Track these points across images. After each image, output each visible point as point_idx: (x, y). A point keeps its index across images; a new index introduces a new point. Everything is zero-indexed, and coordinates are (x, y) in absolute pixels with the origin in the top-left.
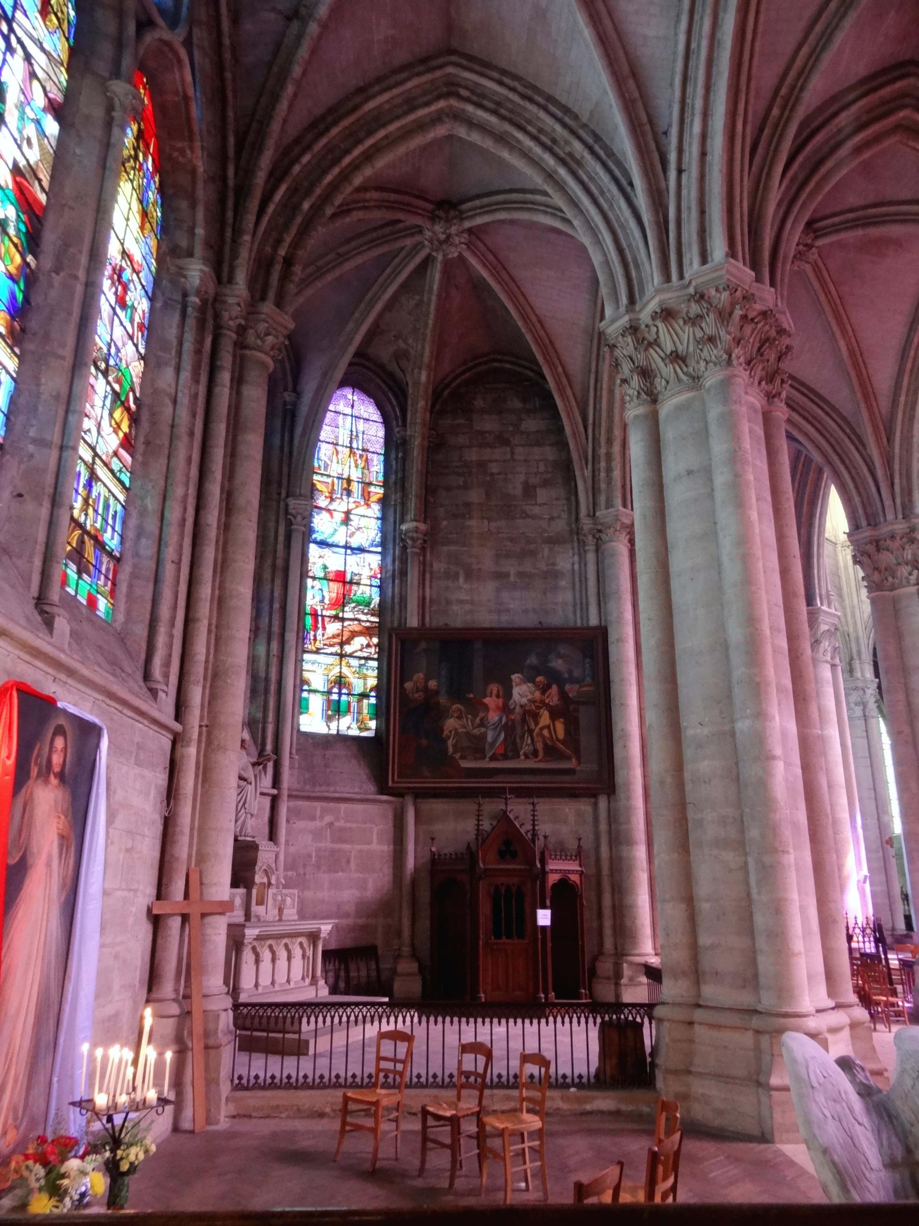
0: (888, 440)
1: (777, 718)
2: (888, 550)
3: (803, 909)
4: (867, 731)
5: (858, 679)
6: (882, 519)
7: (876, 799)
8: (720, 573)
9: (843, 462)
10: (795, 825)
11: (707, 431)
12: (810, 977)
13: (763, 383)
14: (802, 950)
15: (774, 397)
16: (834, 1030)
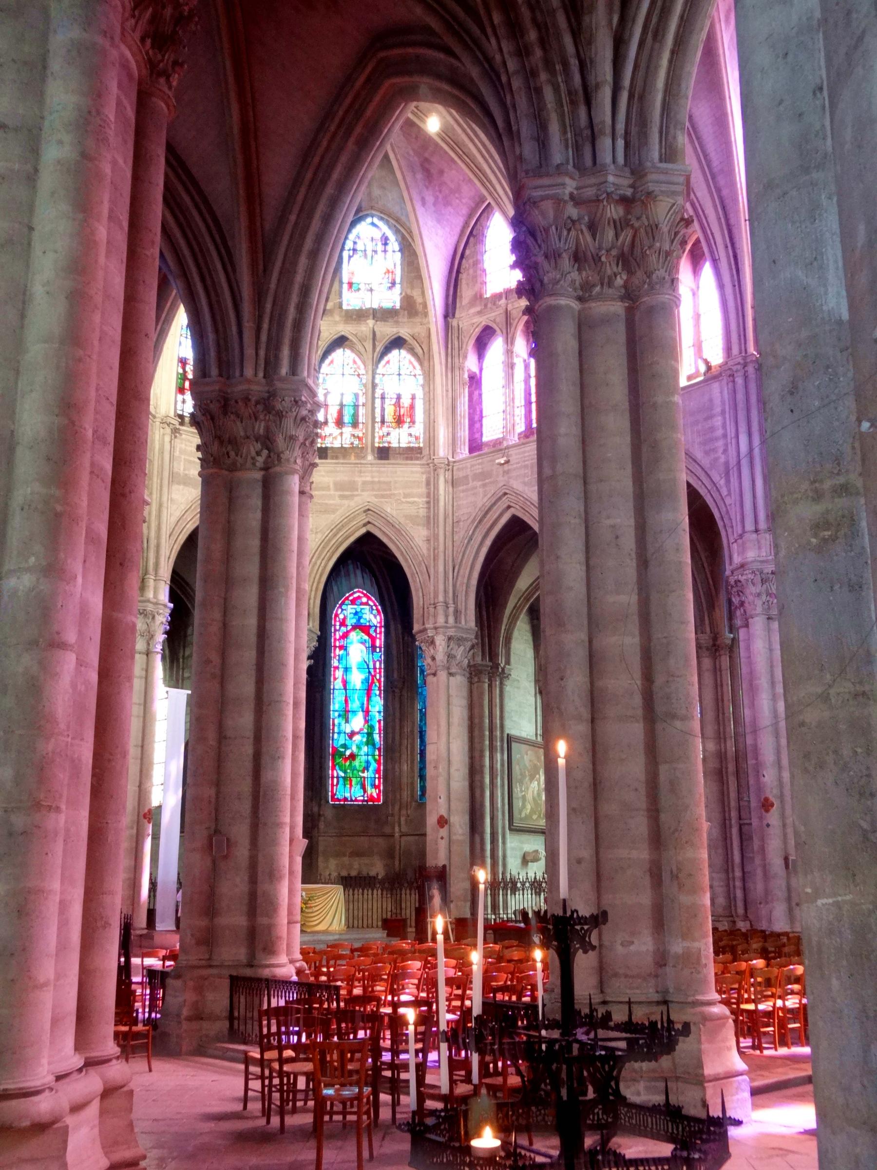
0: (265, 271)
1: (80, 580)
2: (238, 416)
3: (63, 906)
4: (147, 671)
5: (148, 601)
6: (237, 374)
7: (142, 759)
8: (23, 316)
9: (203, 280)
10: (75, 765)
11: (45, 68)
12: (55, 1022)
13: (149, 42)
14: (52, 976)
15: (160, 74)
16: (77, 1108)
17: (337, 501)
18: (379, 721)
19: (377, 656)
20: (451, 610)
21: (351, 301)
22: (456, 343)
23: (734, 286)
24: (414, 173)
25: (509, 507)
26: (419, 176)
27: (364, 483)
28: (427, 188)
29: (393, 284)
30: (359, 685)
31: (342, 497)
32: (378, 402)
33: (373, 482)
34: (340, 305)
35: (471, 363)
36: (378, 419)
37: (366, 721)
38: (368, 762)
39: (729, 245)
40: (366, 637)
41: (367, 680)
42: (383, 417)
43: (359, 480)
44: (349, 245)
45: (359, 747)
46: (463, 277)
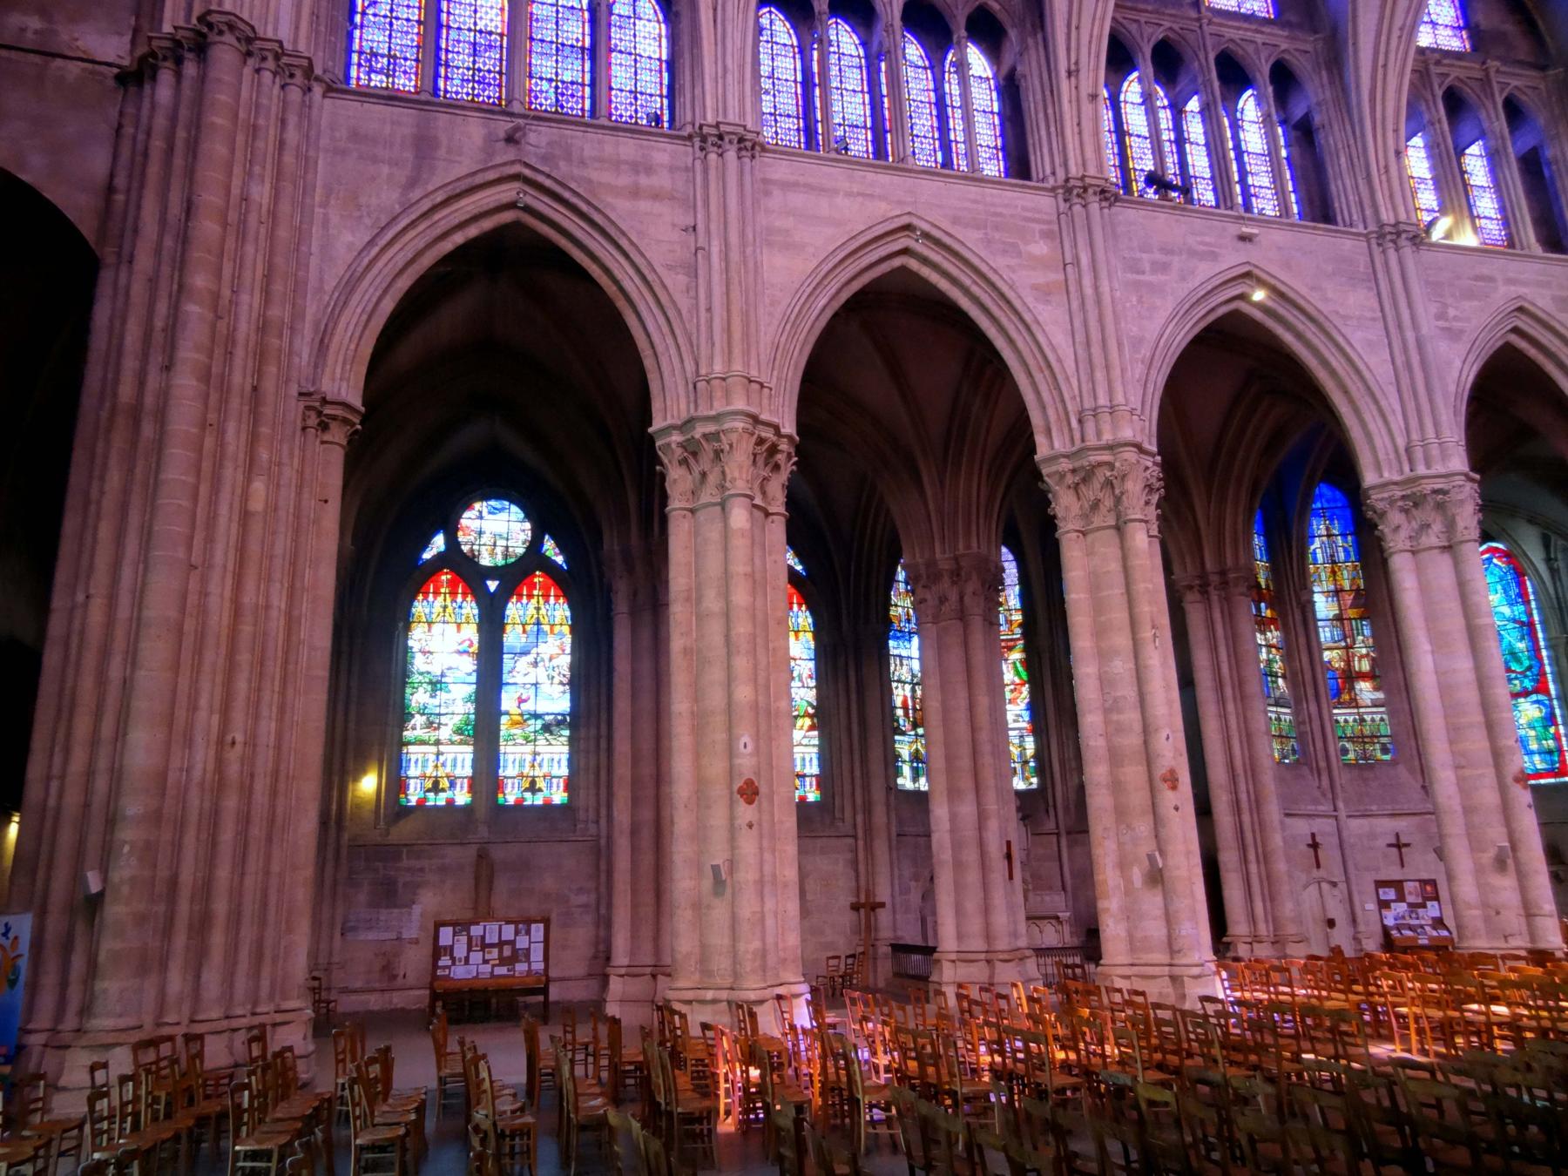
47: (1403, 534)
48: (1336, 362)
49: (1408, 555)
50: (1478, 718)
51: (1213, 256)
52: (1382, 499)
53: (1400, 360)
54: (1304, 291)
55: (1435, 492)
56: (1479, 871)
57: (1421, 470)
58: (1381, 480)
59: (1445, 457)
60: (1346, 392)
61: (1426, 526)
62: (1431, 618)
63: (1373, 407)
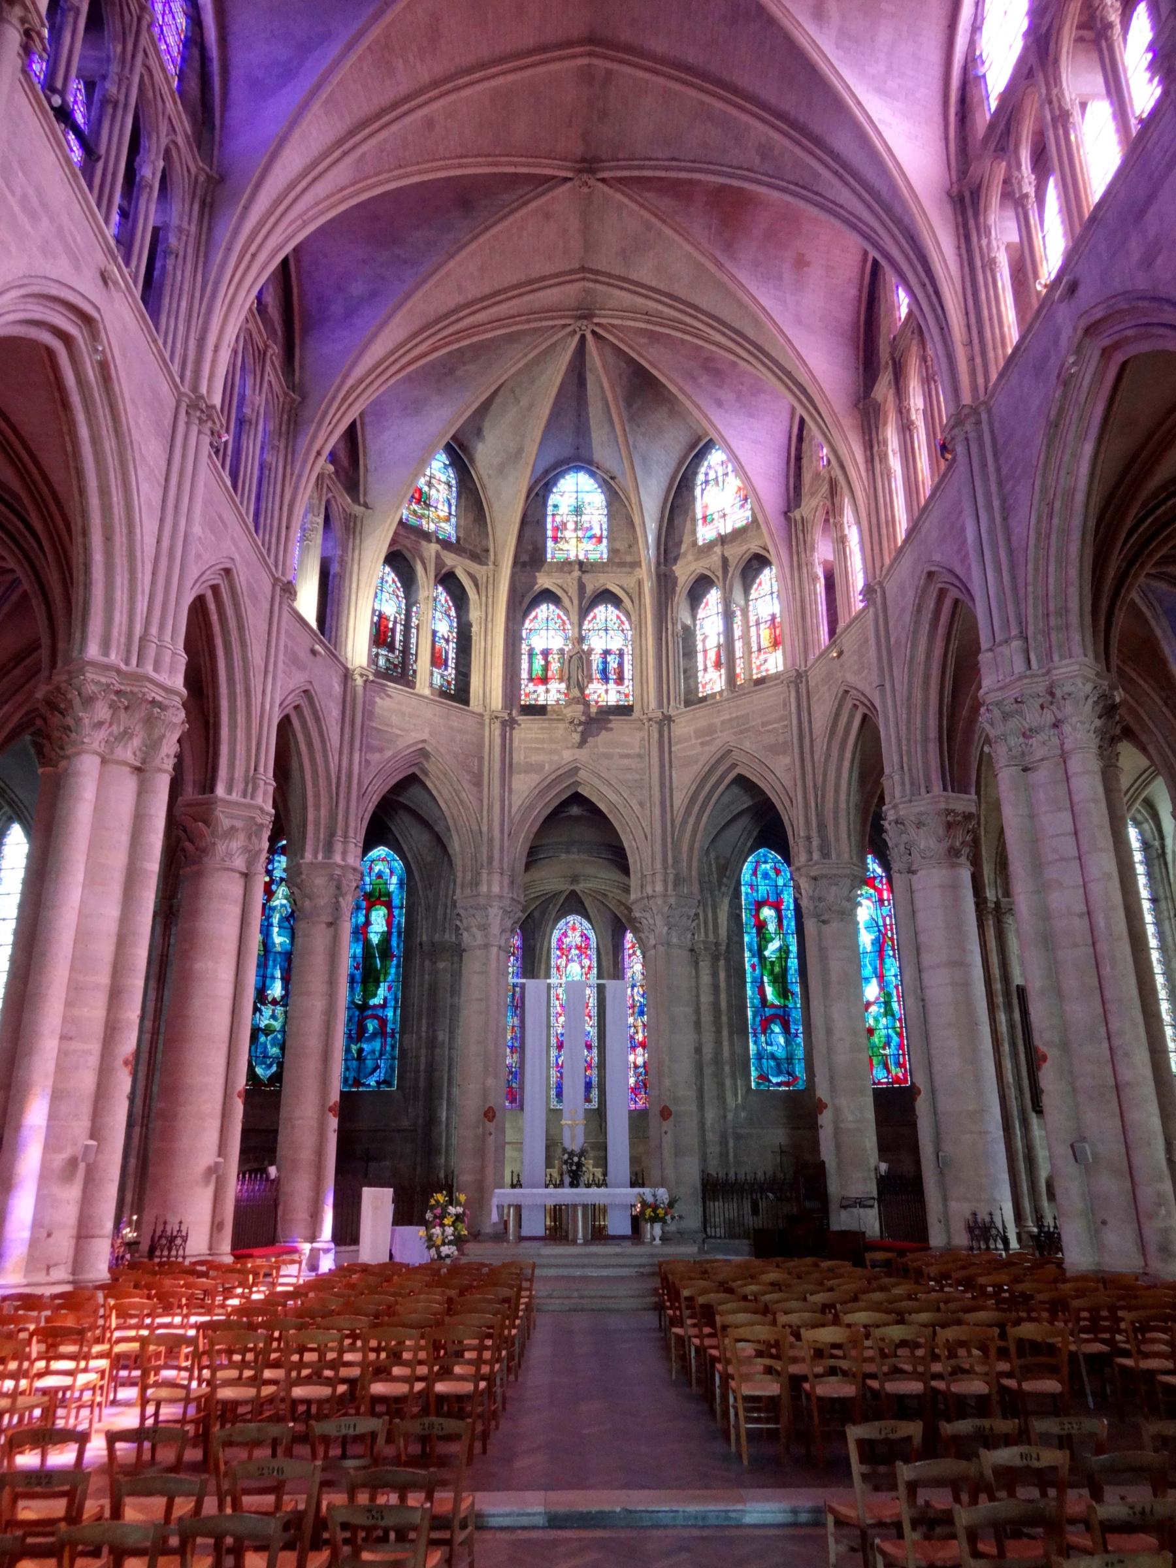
17: (699, 749)
18: (896, 987)
19: (885, 911)
20: (816, 842)
21: (705, 534)
22: (801, 536)
23: (942, 329)
24: (693, 378)
25: (855, 706)
26: (704, 379)
27: (723, 722)
28: (720, 387)
29: (746, 499)
30: (869, 948)
31: (703, 744)
32: (753, 630)
33: (731, 720)
34: (694, 543)
35: (823, 551)
36: (755, 648)
37: (882, 988)
38: (888, 1036)
39: (927, 281)
40: (872, 891)
41: (877, 939)
42: (759, 643)
43: (717, 721)
44: (701, 478)
45: (876, 1020)
46: (805, 462)
47: (102, 734)
48: (117, 498)
49: (98, 760)
50: (104, 979)
51: (77, 268)
52: (98, 683)
53: (166, 543)
54: (127, 396)
55: (153, 702)
56: (44, 1177)
57: (149, 669)
58: (104, 659)
59: (172, 670)
60: (108, 539)
61: (126, 735)
62: (95, 844)
63: (127, 575)
